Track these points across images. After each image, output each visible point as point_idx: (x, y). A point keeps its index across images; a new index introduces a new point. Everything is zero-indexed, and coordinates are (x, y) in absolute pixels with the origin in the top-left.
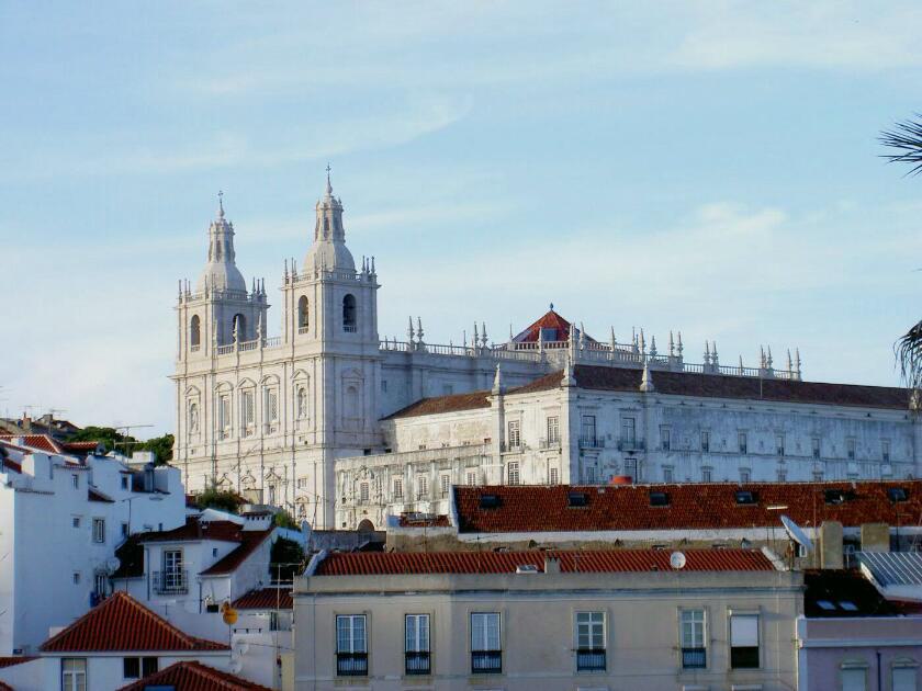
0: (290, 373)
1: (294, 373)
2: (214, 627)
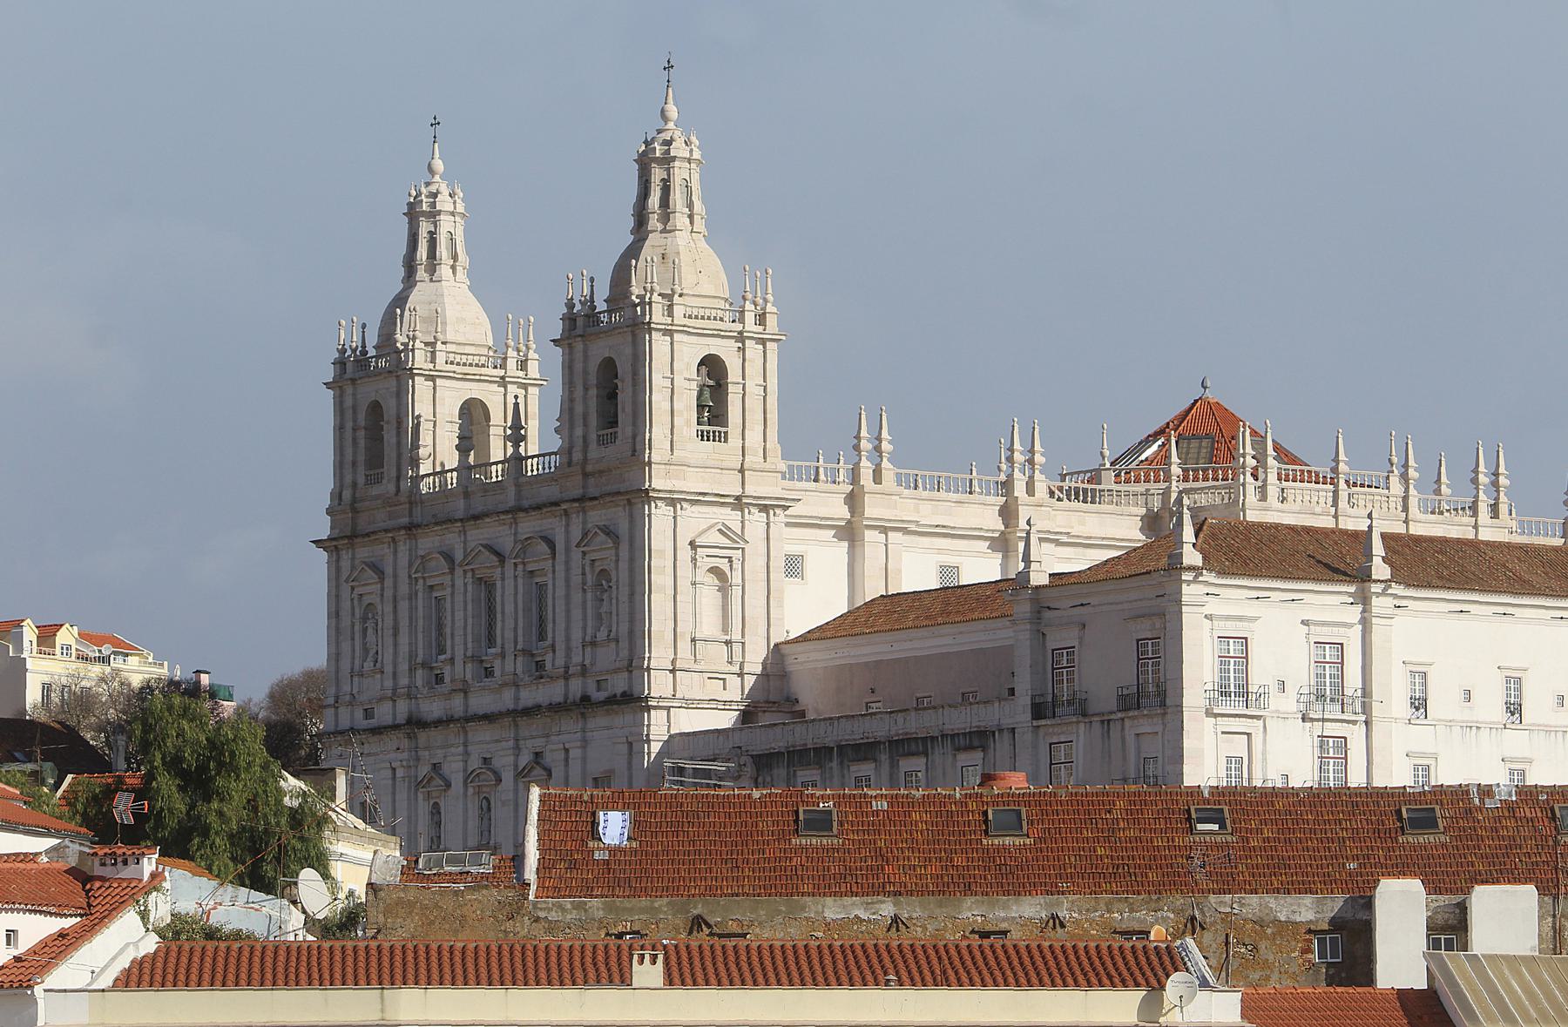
0: (576, 534)
1: (585, 535)
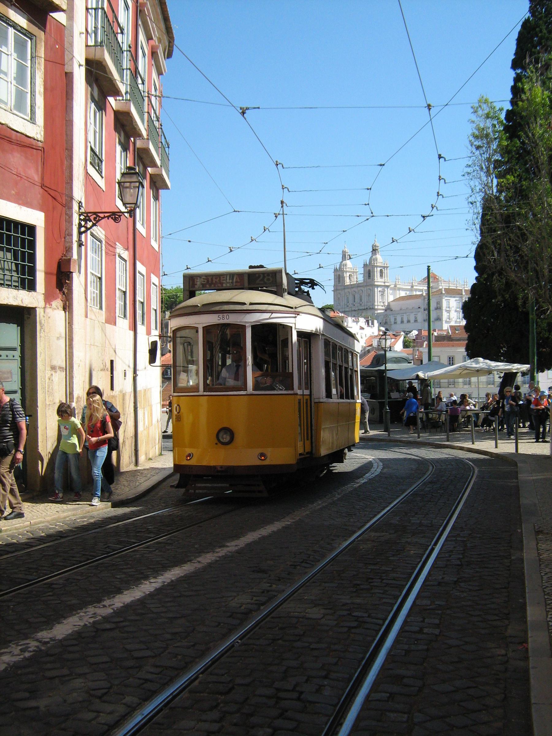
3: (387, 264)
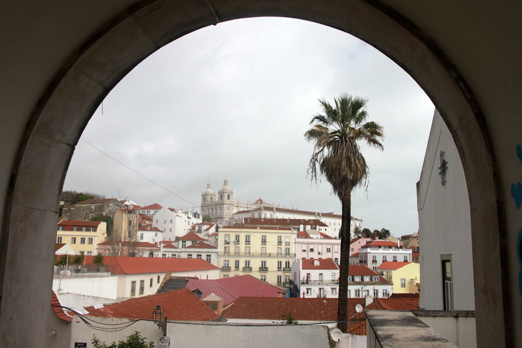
2: (206, 238)
3: (232, 192)
